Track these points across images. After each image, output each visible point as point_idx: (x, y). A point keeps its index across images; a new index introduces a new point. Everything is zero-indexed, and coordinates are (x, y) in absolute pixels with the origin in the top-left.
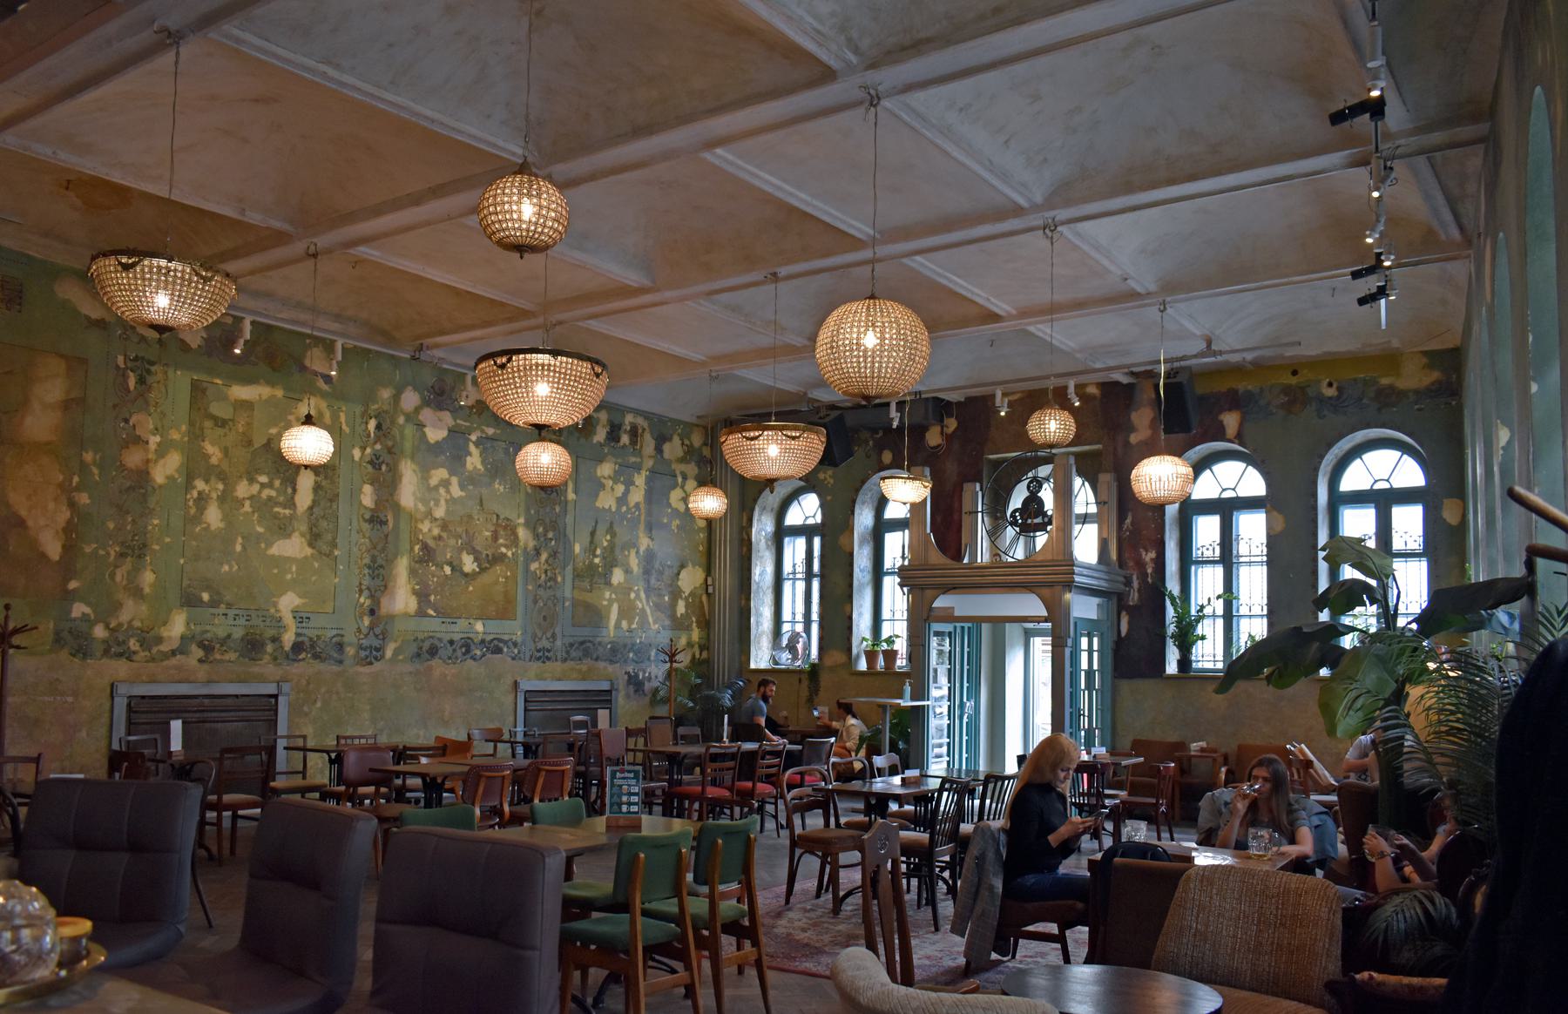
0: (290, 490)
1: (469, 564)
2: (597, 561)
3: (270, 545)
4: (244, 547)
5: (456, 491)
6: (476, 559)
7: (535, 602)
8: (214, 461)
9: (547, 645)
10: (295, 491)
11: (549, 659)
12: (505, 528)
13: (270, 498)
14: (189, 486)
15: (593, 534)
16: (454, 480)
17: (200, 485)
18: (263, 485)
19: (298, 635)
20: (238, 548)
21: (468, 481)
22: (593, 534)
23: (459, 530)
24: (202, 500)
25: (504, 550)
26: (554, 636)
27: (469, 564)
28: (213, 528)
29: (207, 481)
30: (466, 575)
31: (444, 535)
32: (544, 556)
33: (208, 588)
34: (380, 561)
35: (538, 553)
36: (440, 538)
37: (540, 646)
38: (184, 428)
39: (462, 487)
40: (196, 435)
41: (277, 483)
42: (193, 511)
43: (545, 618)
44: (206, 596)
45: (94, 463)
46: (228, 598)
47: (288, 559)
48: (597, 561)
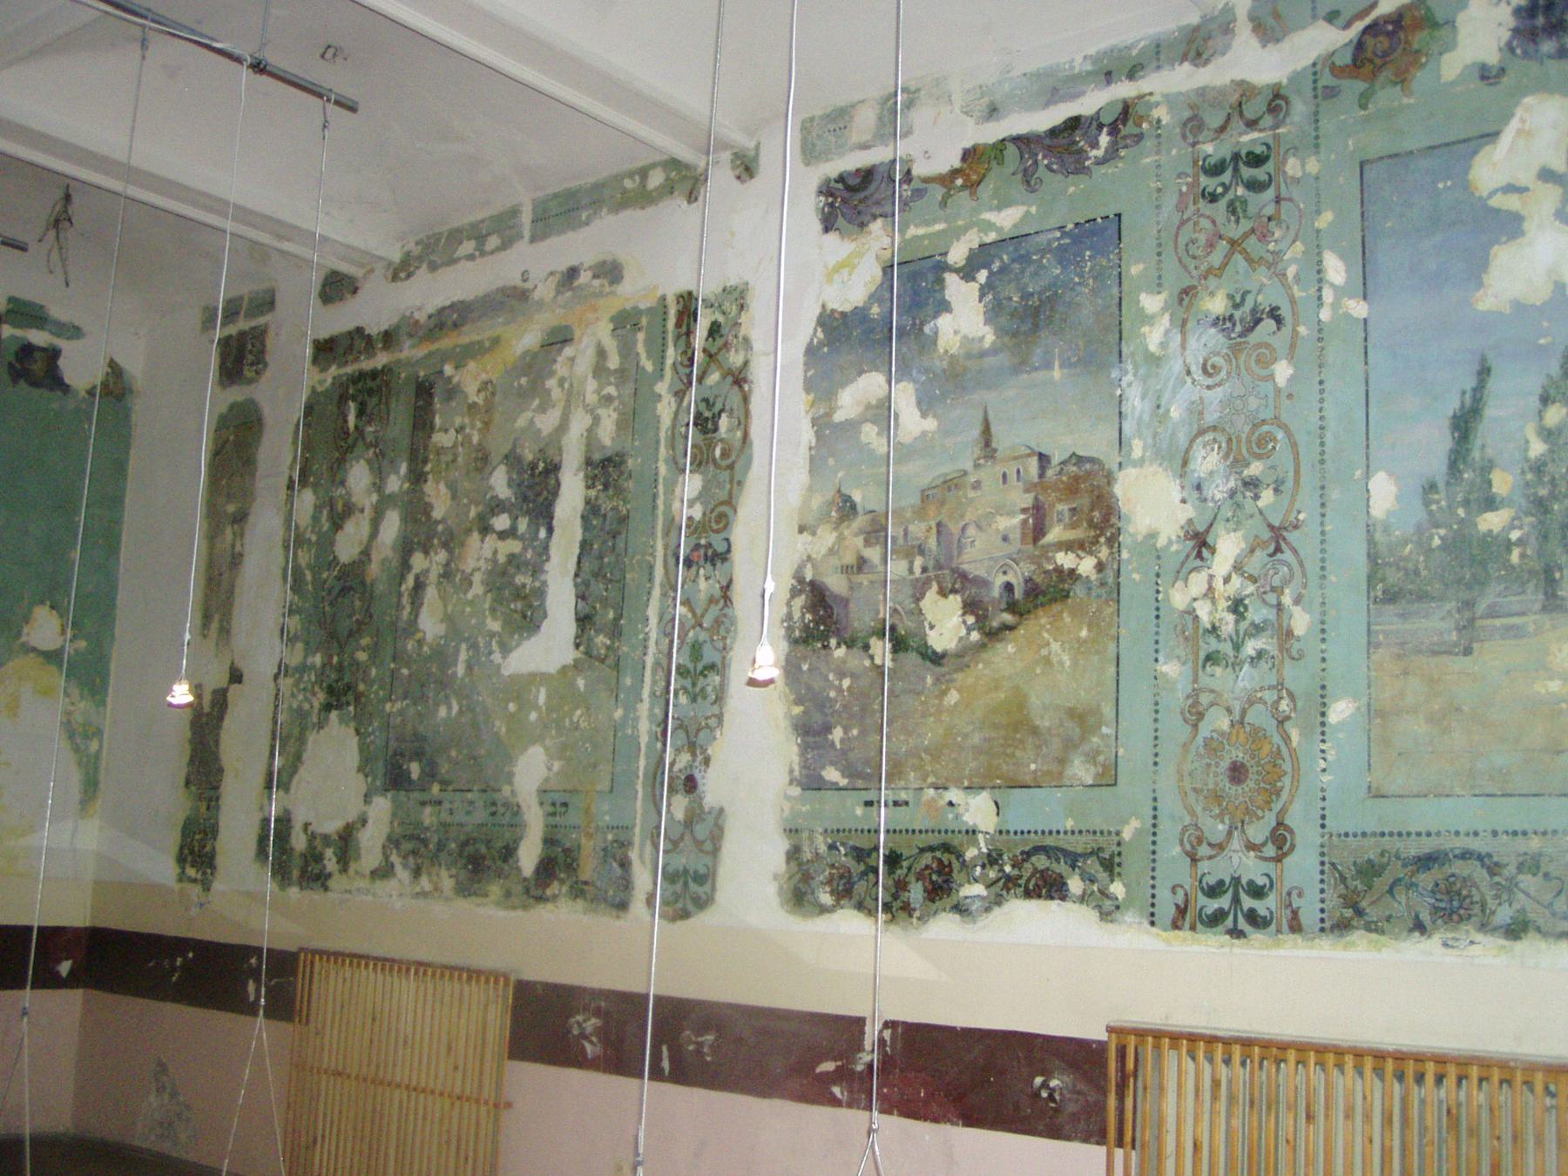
0: (543, 533)
1: (946, 624)
2: (1492, 521)
3: (506, 650)
4: (470, 668)
5: (912, 421)
6: (970, 606)
7: (1195, 715)
8: (437, 514)
9: (1252, 868)
10: (550, 530)
11: (1253, 918)
12: (1072, 489)
13: (512, 558)
14: (405, 566)
15: (1464, 424)
16: (904, 397)
17: (418, 561)
18: (503, 535)
19: (549, 841)
20: (461, 670)
21: (948, 383)
22: (1464, 424)
23: (917, 529)
24: (419, 586)
25: (1065, 560)
26: (1281, 839)
27: (946, 624)
28: (429, 637)
29: (426, 553)
30: (936, 659)
31: (873, 554)
32: (1228, 546)
33: (418, 755)
34: (709, 655)
35: (1200, 543)
36: (862, 564)
37: (1215, 870)
38: (404, 468)
39: (925, 405)
40: (417, 477)
41: (523, 525)
42: (405, 614)
43: (1237, 772)
44: (415, 769)
45: (309, 566)
46: (444, 768)
47: (535, 678)
48: (1492, 521)
